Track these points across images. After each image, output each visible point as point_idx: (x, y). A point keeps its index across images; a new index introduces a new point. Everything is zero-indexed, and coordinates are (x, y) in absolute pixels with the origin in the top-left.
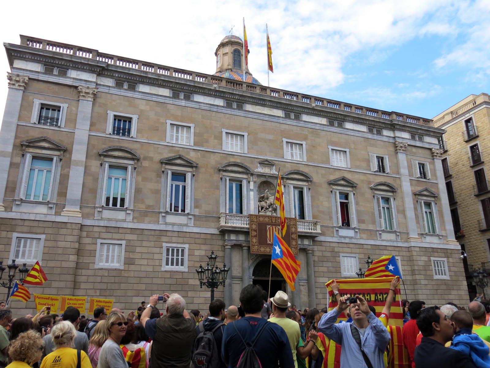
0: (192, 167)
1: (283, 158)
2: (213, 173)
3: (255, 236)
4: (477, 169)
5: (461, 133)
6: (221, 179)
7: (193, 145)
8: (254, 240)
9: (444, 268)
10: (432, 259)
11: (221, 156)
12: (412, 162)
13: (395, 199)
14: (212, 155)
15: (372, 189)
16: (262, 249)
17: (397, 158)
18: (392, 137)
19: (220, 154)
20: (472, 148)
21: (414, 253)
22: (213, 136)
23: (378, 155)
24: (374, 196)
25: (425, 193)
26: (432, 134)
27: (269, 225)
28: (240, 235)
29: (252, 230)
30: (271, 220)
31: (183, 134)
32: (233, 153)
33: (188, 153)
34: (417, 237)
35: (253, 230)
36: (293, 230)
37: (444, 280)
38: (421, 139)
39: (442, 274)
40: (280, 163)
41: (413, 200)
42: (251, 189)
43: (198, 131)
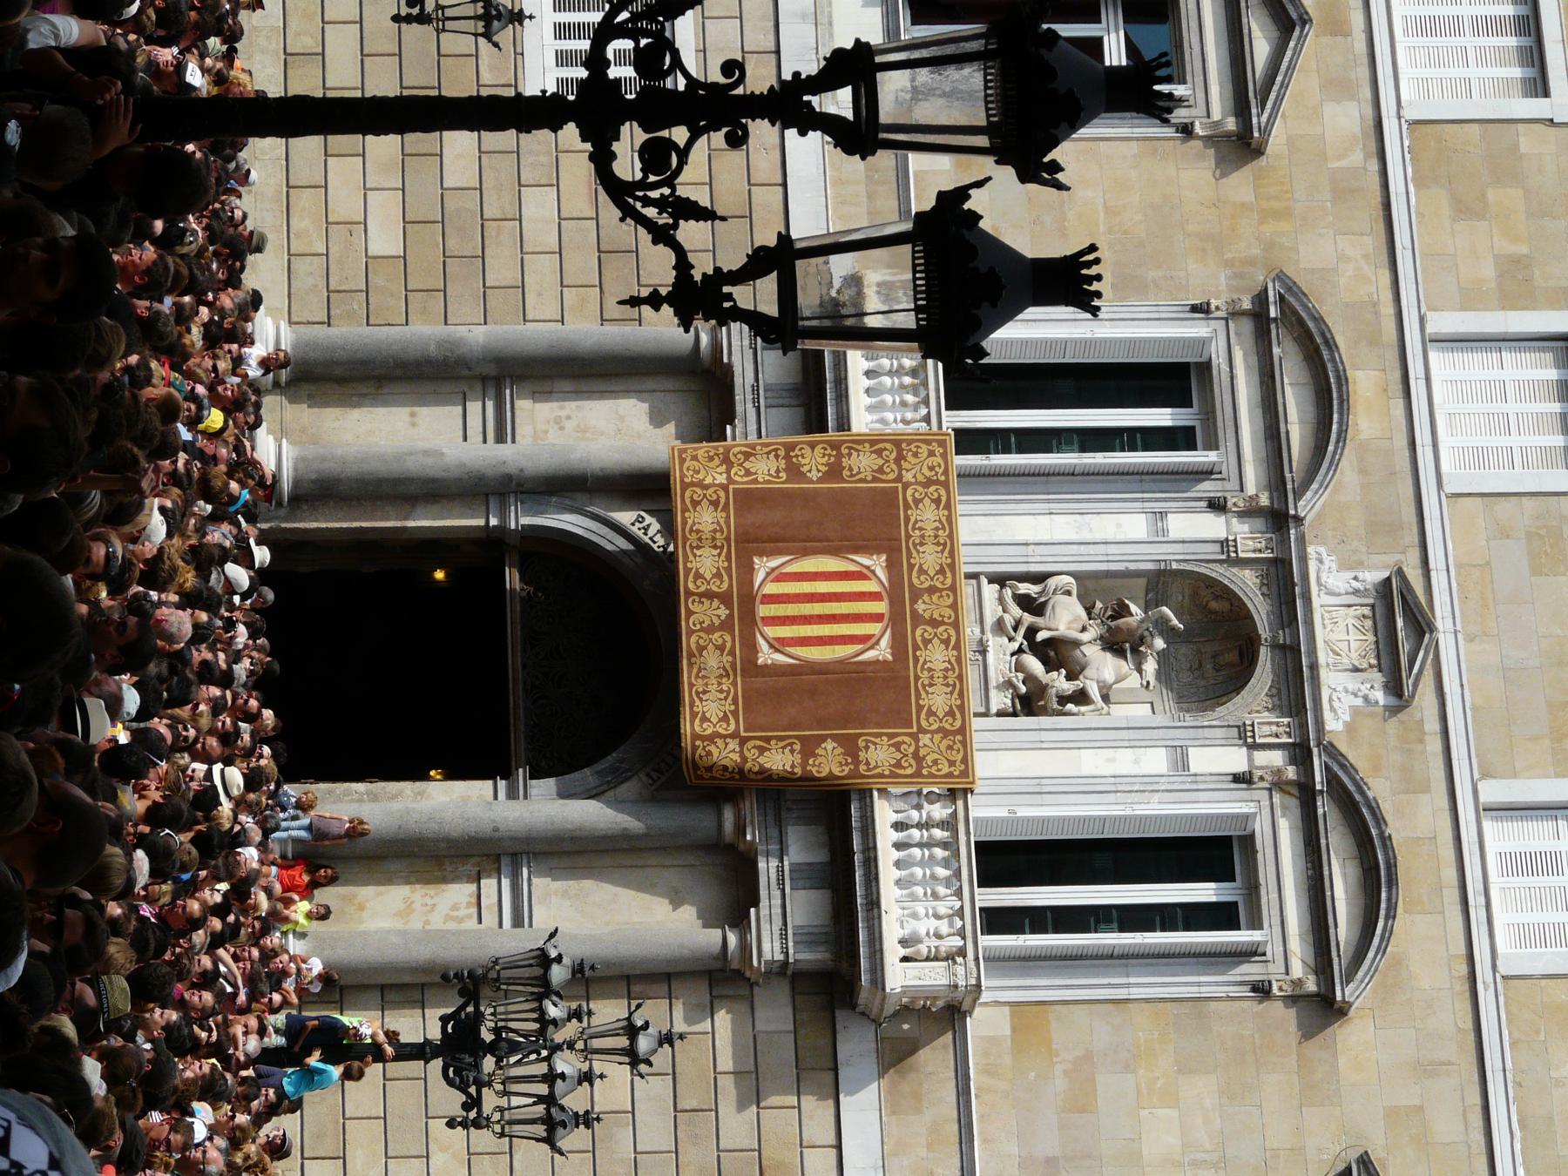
0: (1241, 108)
1: (1486, 775)
2: (1228, 256)
3: (794, 471)
6: (1201, 309)
7: (1410, 114)
8: (765, 469)
11: (1375, 304)
14: (1373, 242)
16: (706, 519)
19: (1387, 295)
22: (1523, 249)
27: (893, 566)
28: (800, 411)
29: (836, 446)
30: (932, 590)
31: (1482, 61)
32: (1418, 388)
33: (1337, 88)
35: (840, 456)
36: (879, 755)
40: (1435, 745)
42: (1162, 515)
43: (1525, 145)
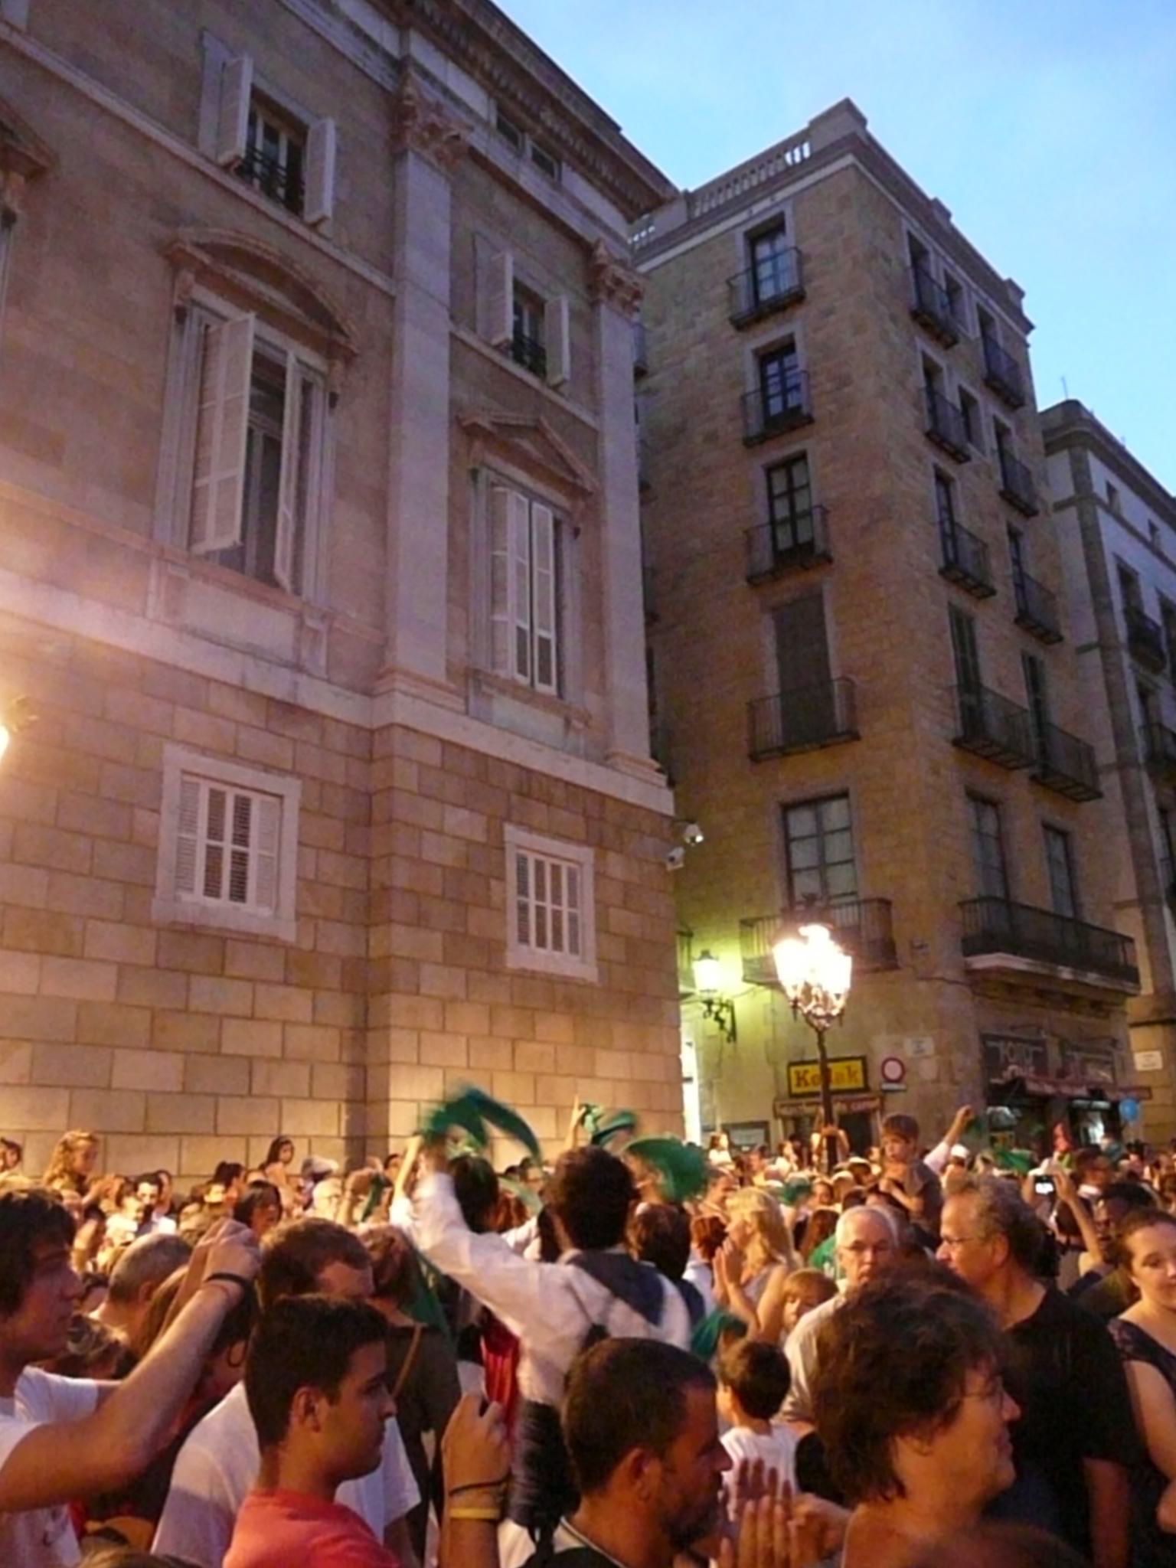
4: (776, 453)
5: (721, 290)
9: (573, 903)
10: (513, 834)
12: (483, 254)
13: (333, 399)
15: (174, 259)
17: (394, 181)
18: (387, 56)
20: (764, 357)
21: (406, 776)
23: (264, 86)
24: (181, 315)
25: (526, 445)
26: (605, 171)
34: (441, 677)
37: (566, 981)
38: (546, 163)
39: (557, 945)
41: (454, 455)
